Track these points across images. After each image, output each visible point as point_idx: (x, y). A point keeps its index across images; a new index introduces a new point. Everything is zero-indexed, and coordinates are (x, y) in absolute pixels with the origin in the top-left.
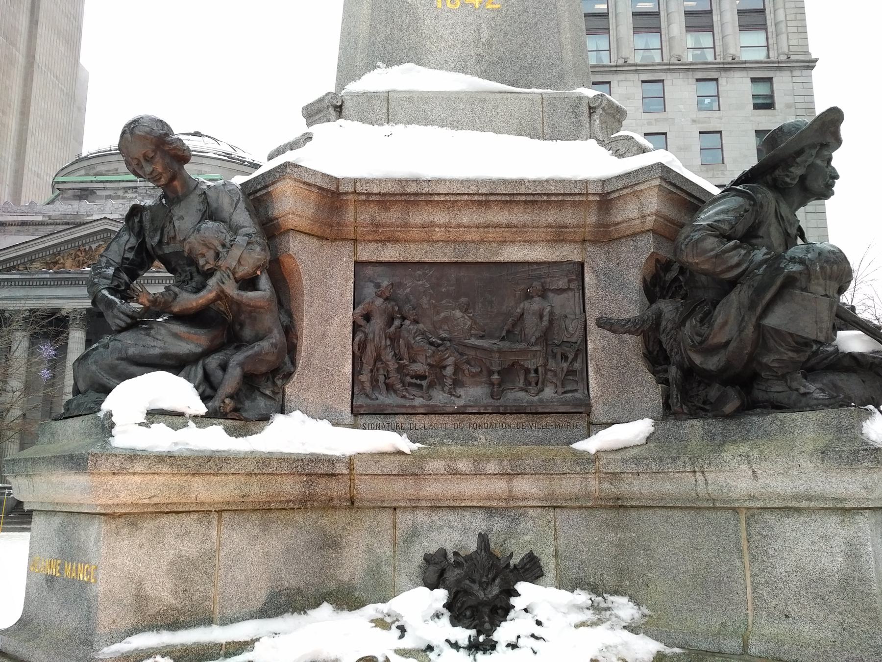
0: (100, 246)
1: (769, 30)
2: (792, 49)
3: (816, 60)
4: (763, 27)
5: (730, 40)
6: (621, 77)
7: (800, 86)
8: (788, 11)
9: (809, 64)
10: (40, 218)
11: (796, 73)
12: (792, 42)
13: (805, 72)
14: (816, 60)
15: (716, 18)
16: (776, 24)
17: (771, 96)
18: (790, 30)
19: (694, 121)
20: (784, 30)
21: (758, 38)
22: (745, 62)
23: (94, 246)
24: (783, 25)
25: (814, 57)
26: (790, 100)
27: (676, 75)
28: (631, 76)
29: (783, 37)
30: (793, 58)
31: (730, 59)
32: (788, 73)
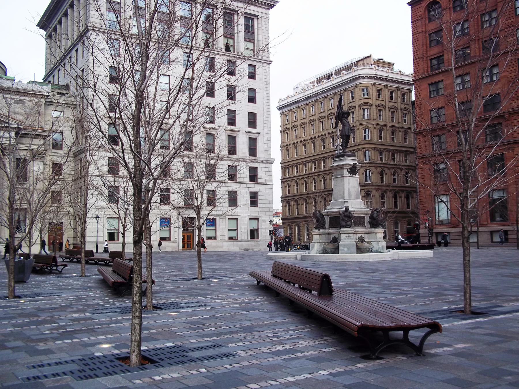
1: (255, 42)
3: (271, 62)
7: (265, 71)
9: (269, 63)
11: (265, 65)
14: (271, 62)
17: (255, 73)
21: (250, 45)
25: (271, 60)
30: (264, 58)
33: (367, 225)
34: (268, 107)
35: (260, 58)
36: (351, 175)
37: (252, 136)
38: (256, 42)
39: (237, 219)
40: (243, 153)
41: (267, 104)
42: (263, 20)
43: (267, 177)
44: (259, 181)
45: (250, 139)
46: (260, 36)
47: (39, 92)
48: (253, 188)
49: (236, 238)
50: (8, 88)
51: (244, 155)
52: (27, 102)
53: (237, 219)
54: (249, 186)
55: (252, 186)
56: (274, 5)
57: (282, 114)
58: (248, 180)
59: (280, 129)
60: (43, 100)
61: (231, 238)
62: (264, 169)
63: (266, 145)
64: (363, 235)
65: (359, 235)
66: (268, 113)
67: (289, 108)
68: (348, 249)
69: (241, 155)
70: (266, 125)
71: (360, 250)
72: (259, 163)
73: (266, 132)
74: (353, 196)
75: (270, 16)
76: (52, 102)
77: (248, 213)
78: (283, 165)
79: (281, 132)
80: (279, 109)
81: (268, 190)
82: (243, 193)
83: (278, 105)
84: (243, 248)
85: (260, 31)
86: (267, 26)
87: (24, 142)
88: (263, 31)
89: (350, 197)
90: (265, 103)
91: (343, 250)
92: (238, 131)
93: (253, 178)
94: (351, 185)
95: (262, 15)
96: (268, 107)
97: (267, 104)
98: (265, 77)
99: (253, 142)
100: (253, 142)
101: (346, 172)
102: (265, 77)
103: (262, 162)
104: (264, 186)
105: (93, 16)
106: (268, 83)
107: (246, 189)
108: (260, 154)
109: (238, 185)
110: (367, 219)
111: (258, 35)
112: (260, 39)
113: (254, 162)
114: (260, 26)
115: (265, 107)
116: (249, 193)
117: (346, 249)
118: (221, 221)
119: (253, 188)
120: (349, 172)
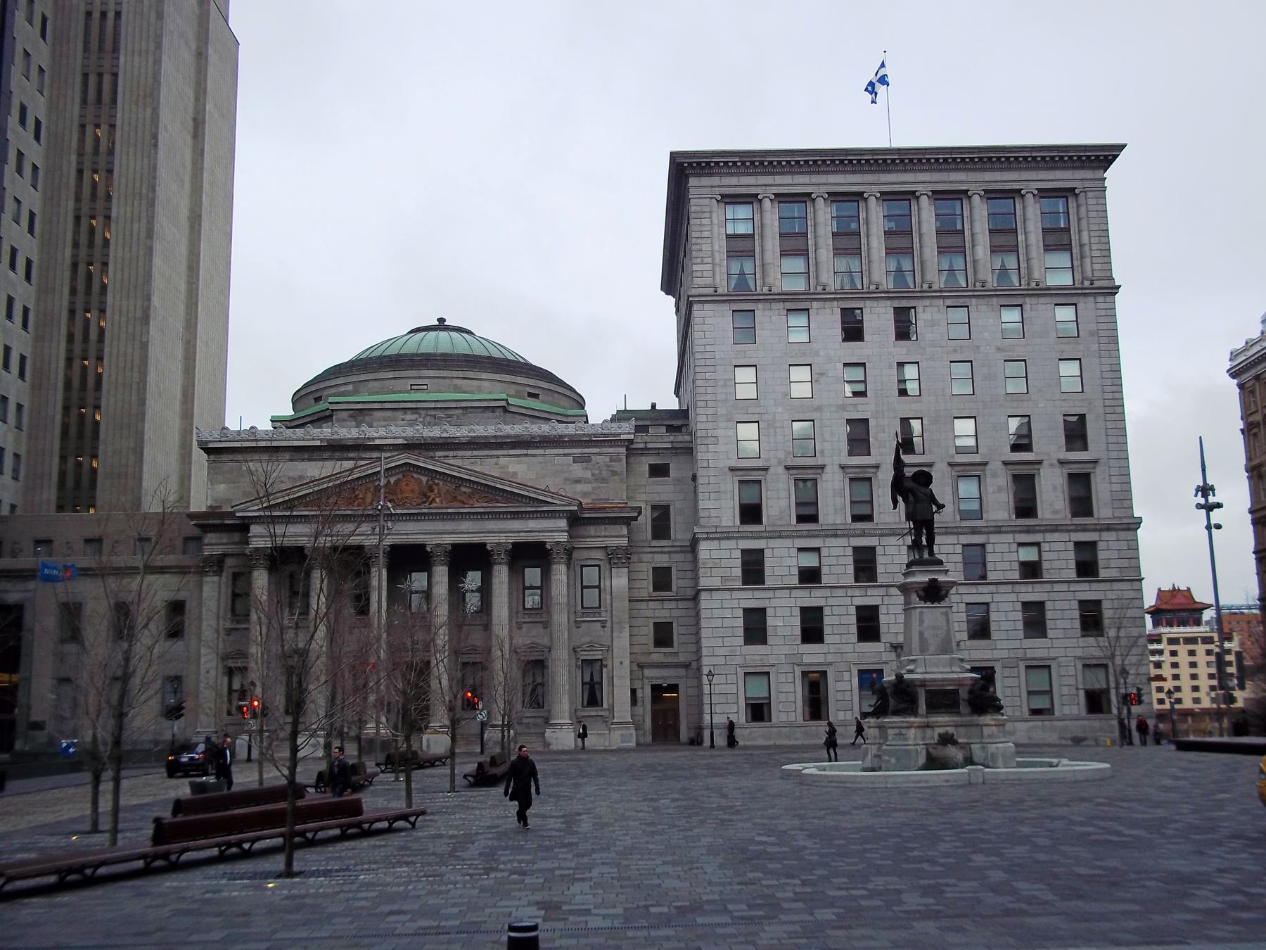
0: (398, 481)
1: (1074, 251)
2: (1096, 274)
4: (1068, 248)
5: (1035, 264)
6: (927, 302)
7: (1103, 312)
8: (1092, 234)
9: (1113, 290)
10: (318, 443)
11: (1100, 299)
12: (1096, 267)
13: (1109, 299)
15: (1021, 238)
16: (1081, 246)
18: (1096, 253)
19: (999, 349)
20: (1088, 253)
21: (1062, 259)
22: (1049, 289)
23: (392, 480)
24: (1087, 248)
26: (1093, 327)
27: (981, 301)
28: (936, 302)
29: (1088, 261)
30: (1097, 284)
31: (1033, 285)
32: (1091, 299)
33: (964, 708)
34: (1117, 396)
35: (1087, 283)
36: (929, 604)
37: (1075, 469)
38: (1076, 250)
39: (1049, 667)
40: (1055, 512)
41: (1114, 388)
42: (1090, 195)
43: (1124, 563)
44: (1103, 574)
45: (1071, 476)
46: (1085, 234)
47: (615, 435)
48: (1088, 591)
49: (1049, 711)
50: (561, 436)
51: (1058, 516)
52: (593, 457)
53: (1049, 667)
54: (1074, 587)
55: (1086, 586)
56: (1115, 157)
57: (1241, 386)
58: (1072, 574)
59: (1241, 425)
60: (623, 450)
61: (1036, 712)
62: (1113, 545)
63: (1116, 487)
64: (950, 730)
65: (942, 730)
66: (1118, 410)
67: (1253, 372)
68: (898, 759)
69: (1049, 516)
70: (1112, 440)
71: (933, 762)
72: (1101, 530)
73: (1114, 455)
74: (932, 649)
75: (1107, 183)
76: (646, 449)
77: (1079, 652)
78: (1259, 515)
79: (1242, 430)
80: (1234, 374)
81: (1132, 594)
82: (1058, 605)
83: (1228, 365)
84: (1069, 736)
85: (1084, 223)
86: (1100, 208)
87: (592, 533)
88: (1092, 221)
89: (923, 650)
90: (1108, 389)
91: (889, 762)
92: (1040, 463)
93: (1087, 568)
94: (926, 624)
95: (1087, 184)
96: (1117, 396)
97: (1114, 388)
98: (1104, 326)
99: (1080, 483)
100: (1080, 483)
101: (914, 597)
102: (1104, 326)
103: (1109, 528)
104: (1116, 586)
105: (699, 274)
106: (1114, 340)
107: (1069, 596)
108: (1103, 510)
109: (1047, 587)
110: (964, 694)
111: (1082, 235)
112: (1085, 239)
113: (1085, 530)
114: (1083, 209)
115: (1110, 396)
116: (1075, 605)
117: (893, 761)
118: (1007, 672)
119: (1088, 591)
120: (920, 598)
